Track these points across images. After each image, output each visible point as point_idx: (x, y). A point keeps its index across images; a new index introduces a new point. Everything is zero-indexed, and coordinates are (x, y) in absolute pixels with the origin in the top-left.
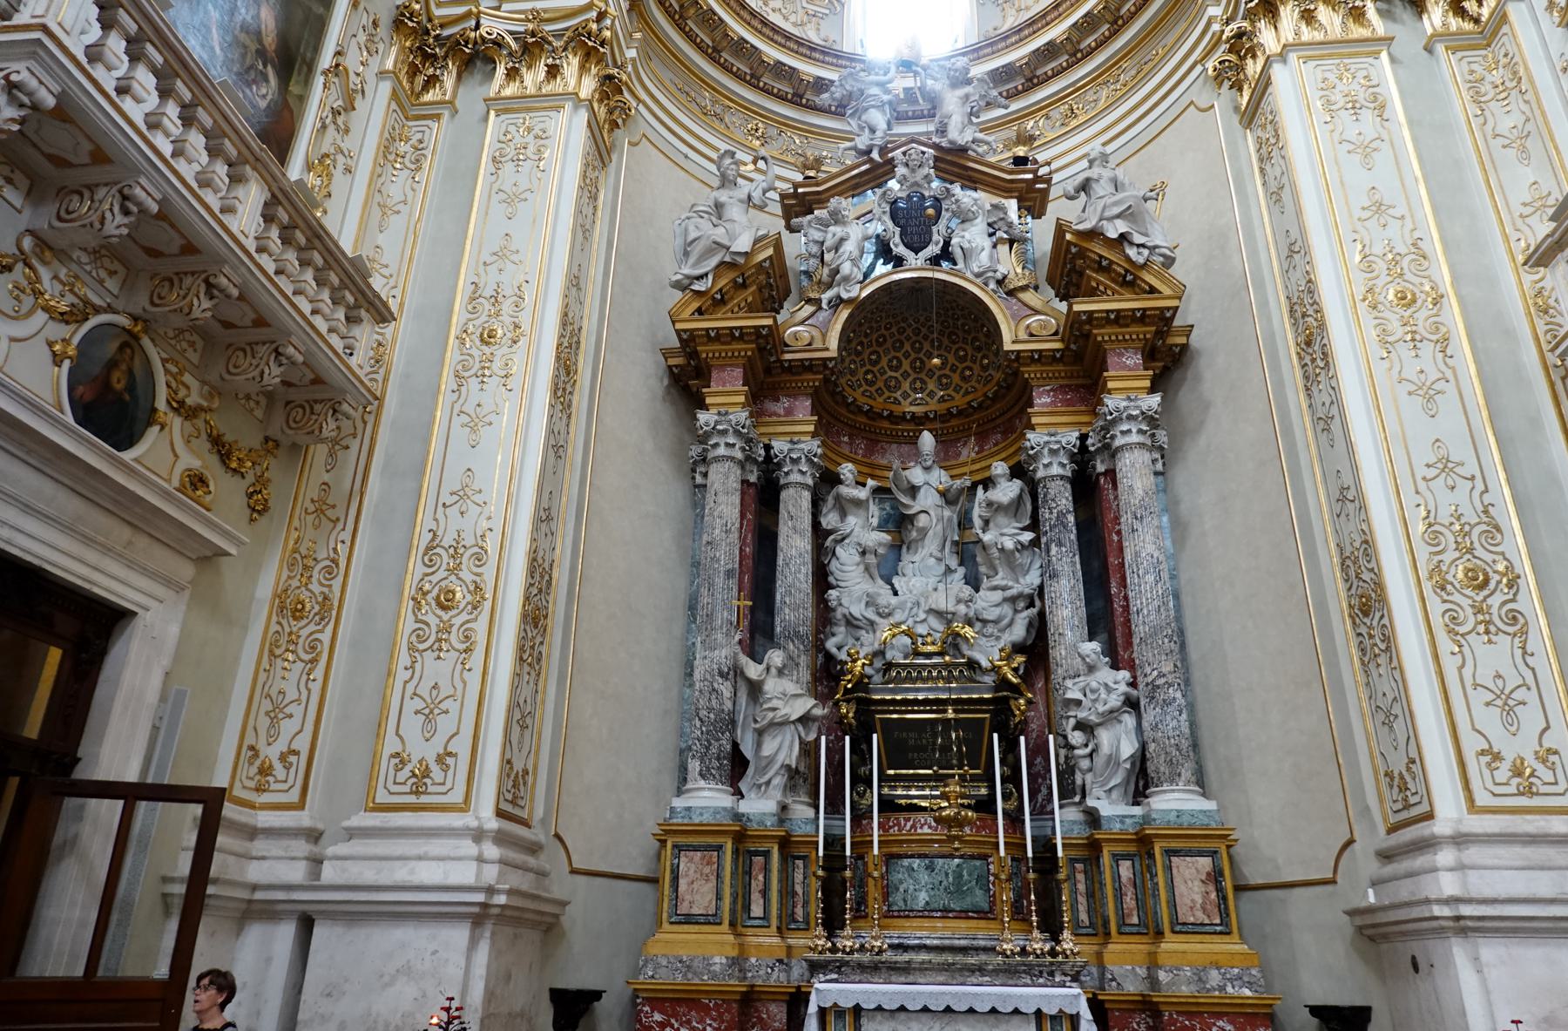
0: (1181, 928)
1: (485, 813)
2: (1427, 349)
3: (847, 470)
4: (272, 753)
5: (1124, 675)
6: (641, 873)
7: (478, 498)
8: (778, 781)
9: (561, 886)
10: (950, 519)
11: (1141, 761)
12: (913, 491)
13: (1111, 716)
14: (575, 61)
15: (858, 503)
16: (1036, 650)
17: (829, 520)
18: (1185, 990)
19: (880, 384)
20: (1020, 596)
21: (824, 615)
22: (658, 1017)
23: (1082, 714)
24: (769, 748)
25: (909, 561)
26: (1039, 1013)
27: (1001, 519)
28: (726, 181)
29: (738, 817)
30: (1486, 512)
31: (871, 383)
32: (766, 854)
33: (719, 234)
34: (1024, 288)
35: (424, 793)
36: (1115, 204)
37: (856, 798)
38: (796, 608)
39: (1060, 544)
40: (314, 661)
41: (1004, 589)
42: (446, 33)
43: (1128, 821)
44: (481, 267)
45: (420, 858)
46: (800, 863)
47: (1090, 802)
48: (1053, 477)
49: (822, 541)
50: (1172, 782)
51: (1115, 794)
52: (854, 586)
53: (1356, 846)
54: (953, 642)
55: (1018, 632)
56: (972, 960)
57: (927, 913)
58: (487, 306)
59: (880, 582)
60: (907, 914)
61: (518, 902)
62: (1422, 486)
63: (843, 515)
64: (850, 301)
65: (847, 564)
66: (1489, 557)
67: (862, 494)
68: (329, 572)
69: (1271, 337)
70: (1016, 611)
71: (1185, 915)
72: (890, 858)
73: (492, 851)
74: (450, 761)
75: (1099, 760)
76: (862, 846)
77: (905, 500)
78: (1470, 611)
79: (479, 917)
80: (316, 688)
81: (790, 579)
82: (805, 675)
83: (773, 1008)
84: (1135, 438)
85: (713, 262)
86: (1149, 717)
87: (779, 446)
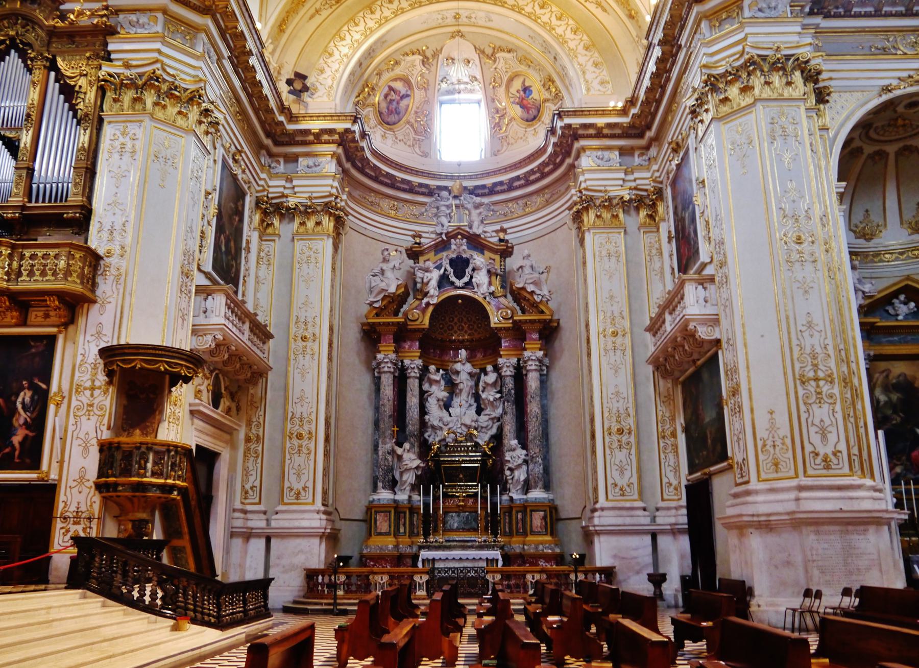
0: (533, 533)
1: (319, 505)
2: (618, 353)
3: (432, 368)
4: (248, 487)
5: (524, 452)
7: (307, 401)
8: (408, 488)
9: (339, 525)
10: (471, 387)
11: (527, 481)
12: (458, 373)
13: (519, 466)
14: (327, 219)
15: (438, 382)
16: (498, 438)
17: (426, 387)
18: (532, 551)
23: (510, 465)
24: (405, 477)
25: (456, 401)
27: (489, 388)
28: (385, 260)
29: (395, 501)
32: (405, 513)
33: (383, 285)
38: (413, 425)
39: (508, 402)
40: (257, 457)
42: (274, 201)
49: (423, 396)
50: (535, 488)
52: (435, 414)
55: (494, 431)
56: (469, 544)
57: (457, 530)
60: (452, 530)
63: (431, 385)
67: (437, 377)
68: (258, 426)
71: (534, 529)
72: (446, 513)
73: (324, 517)
76: (436, 509)
77: (454, 377)
79: (321, 536)
80: (259, 465)
82: (417, 449)
83: (408, 560)
84: (533, 367)
85: (382, 296)
86: (531, 467)
87: (407, 362)
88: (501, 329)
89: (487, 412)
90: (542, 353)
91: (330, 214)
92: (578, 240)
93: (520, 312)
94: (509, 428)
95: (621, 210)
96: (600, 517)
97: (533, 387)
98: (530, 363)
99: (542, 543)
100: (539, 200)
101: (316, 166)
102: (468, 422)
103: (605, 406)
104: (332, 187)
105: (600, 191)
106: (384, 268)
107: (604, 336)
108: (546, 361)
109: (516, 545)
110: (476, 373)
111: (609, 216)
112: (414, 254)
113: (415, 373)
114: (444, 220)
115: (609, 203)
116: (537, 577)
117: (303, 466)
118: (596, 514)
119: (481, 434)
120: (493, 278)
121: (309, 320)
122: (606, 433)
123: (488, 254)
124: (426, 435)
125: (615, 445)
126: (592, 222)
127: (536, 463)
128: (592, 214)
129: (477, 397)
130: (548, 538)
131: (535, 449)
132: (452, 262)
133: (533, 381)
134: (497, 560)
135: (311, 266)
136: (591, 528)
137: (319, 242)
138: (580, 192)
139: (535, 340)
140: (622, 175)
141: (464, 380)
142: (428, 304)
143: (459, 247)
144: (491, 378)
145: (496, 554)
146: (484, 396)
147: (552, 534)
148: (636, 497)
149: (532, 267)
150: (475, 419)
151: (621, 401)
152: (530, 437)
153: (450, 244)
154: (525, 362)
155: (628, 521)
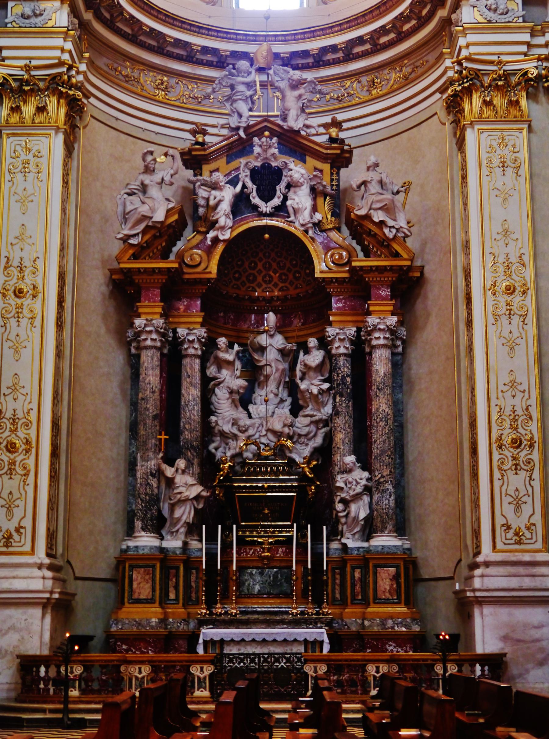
0: (378, 601)
1: (41, 556)
3: (222, 341)
5: (366, 474)
6: (108, 577)
8: (182, 530)
9: (73, 586)
10: (283, 371)
11: (369, 519)
12: (262, 349)
13: (357, 497)
14: (54, 100)
15: (230, 364)
16: (325, 453)
17: (212, 371)
19: (244, 279)
20: (320, 420)
21: (208, 431)
22: (124, 647)
23: (343, 495)
24: (177, 514)
25: (259, 394)
26: (305, 640)
28: (148, 170)
29: (162, 550)
30: (527, 409)
31: (237, 279)
32: (177, 569)
33: (144, 210)
34: (330, 229)
35: (11, 546)
36: (378, 201)
37: (224, 537)
38: (191, 431)
39: (341, 396)
41: (311, 416)
43: (361, 550)
44: (10, 247)
45: (14, 578)
46: (194, 571)
47: (344, 541)
48: (340, 355)
49: (208, 386)
50: (382, 531)
51: (357, 536)
52: (226, 414)
53: (463, 563)
54: (280, 450)
55: (319, 441)
57: (260, 595)
58: (17, 273)
59: (241, 409)
60: (251, 596)
61: (63, 597)
62: (500, 394)
63: (219, 369)
64: (224, 241)
66: (523, 432)
67: (230, 356)
69: (456, 288)
70: (318, 429)
72: (241, 569)
73: (49, 574)
74: (22, 530)
75: (350, 520)
76: (226, 562)
78: (510, 459)
79: (45, 605)
81: (188, 414)
82: (196, 469)
83: (181, 642)
84: (382, 342)
85: (142, 226)
86: (376, 497)
87: (182, 331)
88: (330, 281)
89: (308, 411)
90: (395, 319)
91: (61, 95)
92: (454, 141)
93: (361, 255)
94: (342, 437)
95: (524, 94)
96: (482, 576)
97: (381, 373)
98: (377, 335)
99: (391, 616)
100: (393, 76)
101: (36, 15)
102: (278, 427)
103: (493, 404)
104: (63, 50)
105: (491, 63)
106: (147, 182)
107: (494, 294)
108: (402, 332)
109: (352, 619)
110: (291, 351)
111: (504, 102)
112: (194, 160)
113: (194, 349)
114: (242, 107)
115: (505, 82)
116: (384, 668)
117: (16, 495)
118: (478, 572)
119: (298, 446)
120: (320, 200)
121: (26, 263)
122: (494, 446)
123: (311, 161)
124: (212, 447)
125: (509, 464)
126: (476, 112)
127: (384, 491)
128: (477, 99)
129: (292, 388)
130: (402, 609)
131: (383, 472)
132: (255, 174)
133: (380, 364)
134: (322, 643)
135: (30, 177)
136: (469, 594)
137: (43, 139)
138: (459, 63)
139: (384, 299)
140: (526, 37)
141: (271, 360)
142: (216, 240)
143: (265, 150)
144: (315, 358)
145: (320, 633)
146: (303, 386)
147: (407, 604)
148: (539, 545)
149: (381, 183)
150: (289, 421)
151: (519, 395)
152: (376, 451)
153: (252, 145)
154: (369, 333)
155: (527, 582)
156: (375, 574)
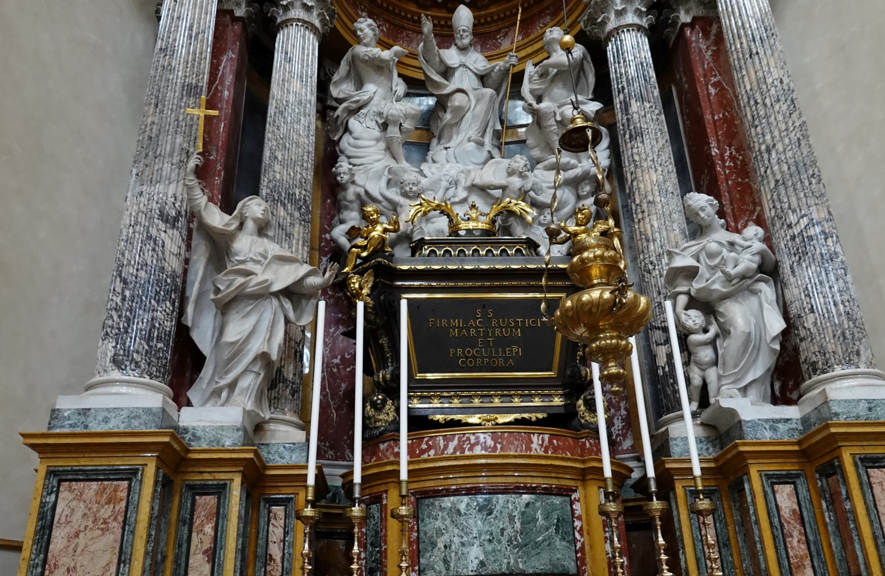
8: (250, 382)
12: (447, 72)
24: (235, 330)
29: (177, 432)
32: (220, 490)
37: (371, 412)
43: (780, 426)
46: (279, 510)
51: (753, 393)
65: (362, 133)
70: (579, 198)
75: (730, 347)
81: (283, 130)
156: (867, 486)
